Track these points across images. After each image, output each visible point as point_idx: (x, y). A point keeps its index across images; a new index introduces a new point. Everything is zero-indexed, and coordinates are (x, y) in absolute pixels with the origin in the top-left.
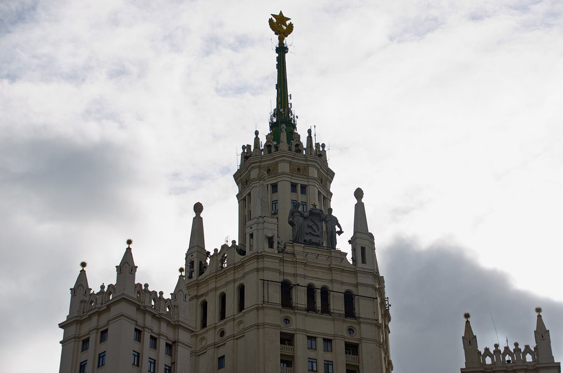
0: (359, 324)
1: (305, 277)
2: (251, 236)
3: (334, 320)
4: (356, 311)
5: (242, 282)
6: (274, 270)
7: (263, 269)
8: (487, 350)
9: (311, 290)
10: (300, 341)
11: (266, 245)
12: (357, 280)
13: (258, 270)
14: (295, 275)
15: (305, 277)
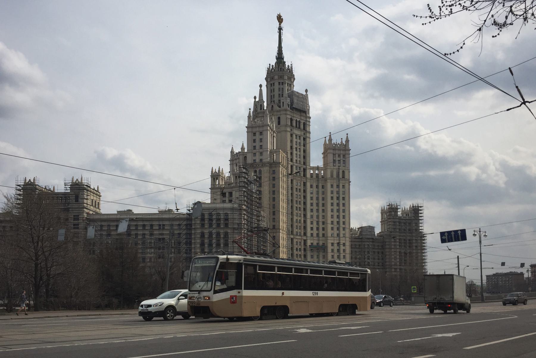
0: (306, 133)
1: (295, 117)
2: (283, 102)
3: (301, 131)
4: (306, 128)
5: (280, 116)
6: (290, 115)
7: (287, 114)
8: (334, 143)
9: (296, 120)
10: (294, 136)
11: (288, 107)
12: (306, 119)
13: (285, 114)
14: (293, 116)
15: (295, 117)
